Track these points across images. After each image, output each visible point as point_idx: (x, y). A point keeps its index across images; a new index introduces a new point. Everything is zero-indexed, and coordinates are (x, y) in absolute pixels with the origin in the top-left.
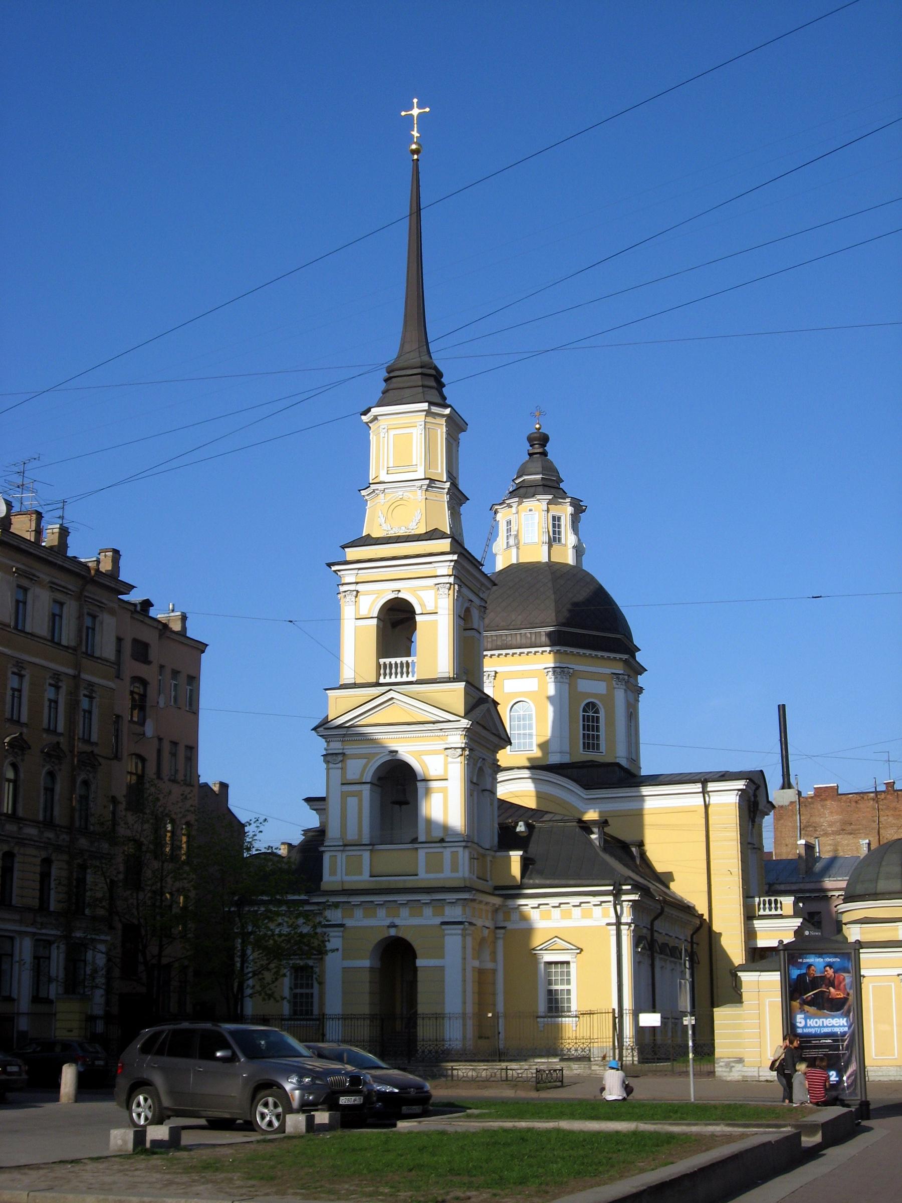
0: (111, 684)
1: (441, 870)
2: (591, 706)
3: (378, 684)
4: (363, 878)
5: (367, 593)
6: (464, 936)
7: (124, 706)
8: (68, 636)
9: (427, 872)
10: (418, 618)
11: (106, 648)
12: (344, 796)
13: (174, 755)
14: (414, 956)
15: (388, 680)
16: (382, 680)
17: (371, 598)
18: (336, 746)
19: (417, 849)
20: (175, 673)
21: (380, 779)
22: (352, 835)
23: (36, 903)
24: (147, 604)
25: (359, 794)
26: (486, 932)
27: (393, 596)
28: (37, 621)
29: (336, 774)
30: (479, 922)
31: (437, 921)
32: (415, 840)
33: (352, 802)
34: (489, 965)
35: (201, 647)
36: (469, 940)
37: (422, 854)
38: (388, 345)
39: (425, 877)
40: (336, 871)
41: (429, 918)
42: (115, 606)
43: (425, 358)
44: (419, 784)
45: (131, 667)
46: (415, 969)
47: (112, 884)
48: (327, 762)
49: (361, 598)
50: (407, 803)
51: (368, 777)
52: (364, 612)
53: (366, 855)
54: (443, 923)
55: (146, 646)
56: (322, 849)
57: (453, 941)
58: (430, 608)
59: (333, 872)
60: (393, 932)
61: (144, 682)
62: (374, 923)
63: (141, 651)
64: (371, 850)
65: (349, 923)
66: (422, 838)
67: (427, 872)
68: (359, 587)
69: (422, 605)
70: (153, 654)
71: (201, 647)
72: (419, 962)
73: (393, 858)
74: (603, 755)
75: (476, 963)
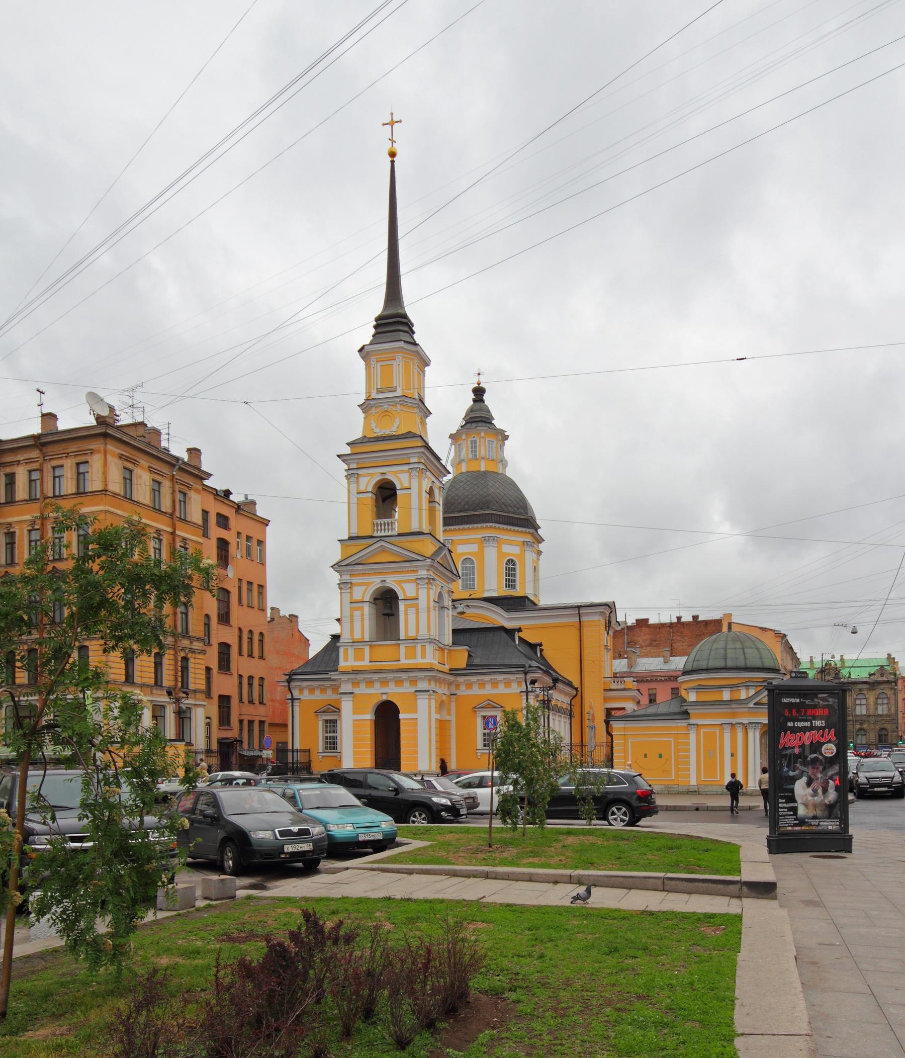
0: (200, 540)
1: (415, 657)
3: (372, 537)
4: (365, 663)
5: (365, 475)
6: (430, 699)
9: (406, 658)
10: (398, 492)
11: (196, 517)
12: (352, 610)
14: (397, 711)
15: (379, 534)
16: (375, 534)
17: (368, 478)
18: (347, 578)
19: (399, 645)
21: (375, 599)
22: (357, 636)
23: (152, 682)
25: (362, 609)
26: (444, 697)
27: (380, 478)
29: (347, 597)
30: (440, 692)
31: (413, 689)
32: (399, 639)
33: (357, 614)
34: (448, 718)
36: (433, 702)
37: (402, 648)
39: (404, 662)
40: (347, 660)
41: (407, 688)
42: (200, 488)
44: (400, 602)
46: (398, 721)
47: (208, 669)
48: (341, 589)
49: (361, 479)
50: (392, 615)
51: (368, 598)
52: (362, 489)
53: (367, 649)
54: (416, 691)
56: (338, 644)
57: (423, 703)
58: (406, 485)
59: (346, 659)
60: (385, 698)
62: (378, 692)
64: (371, 646)
65: (357, 691)
66: (402, 636)
67: (406, 658)
68: (361, 472)
69: (401, 483)
70: (232, 523)
72: (401, 716)
73: (385, 649)
75: (438, 716)
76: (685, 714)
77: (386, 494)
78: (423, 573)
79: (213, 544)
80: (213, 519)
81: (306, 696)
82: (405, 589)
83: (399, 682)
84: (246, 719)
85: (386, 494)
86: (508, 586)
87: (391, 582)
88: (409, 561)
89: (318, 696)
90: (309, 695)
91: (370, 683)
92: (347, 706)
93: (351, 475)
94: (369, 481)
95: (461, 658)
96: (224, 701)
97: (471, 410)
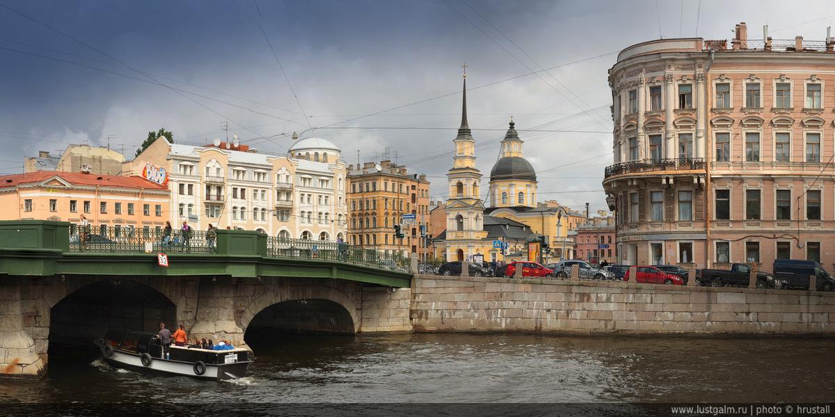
2: (521, 193)
4: (453, 238)
7: (410, 201)
8: (396, 190)
13: (423, 209)
20: (423, 190)
24: (416, 175)
28: (390, 188)
35: (429, 183)
38: (459, 126)
39: (465, 237)
40: (449, 236)
43: (466, 128)
45: (411, 192)
55: (415, 186)
61: (415, 194)
63: (413, 187)
71: (429, 183)
73: (460, 234)
74: (525, 205)
76: (521, 255)
77: (460, 186)
78: (469, 211)
79: (410, 196)
80: (410, 188)
81: (438, 246)
82: (464, 214)
83: (463, 243)
84: (422, 253)
85: (460, 186)
86: (520, 202)
87: (461, 213)
88: (466, 206)
89: (442, 246)
90: (439, 246)
91: (455, 244)
92: (448, 250)
93: (450, 180)
94: (455, 182)
95: (485, 235)
96: (414, 247)
97: (508, 132)
